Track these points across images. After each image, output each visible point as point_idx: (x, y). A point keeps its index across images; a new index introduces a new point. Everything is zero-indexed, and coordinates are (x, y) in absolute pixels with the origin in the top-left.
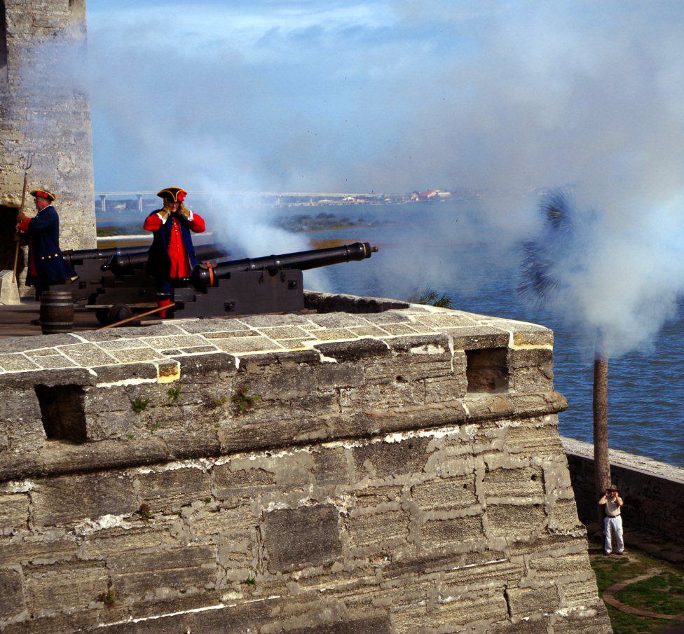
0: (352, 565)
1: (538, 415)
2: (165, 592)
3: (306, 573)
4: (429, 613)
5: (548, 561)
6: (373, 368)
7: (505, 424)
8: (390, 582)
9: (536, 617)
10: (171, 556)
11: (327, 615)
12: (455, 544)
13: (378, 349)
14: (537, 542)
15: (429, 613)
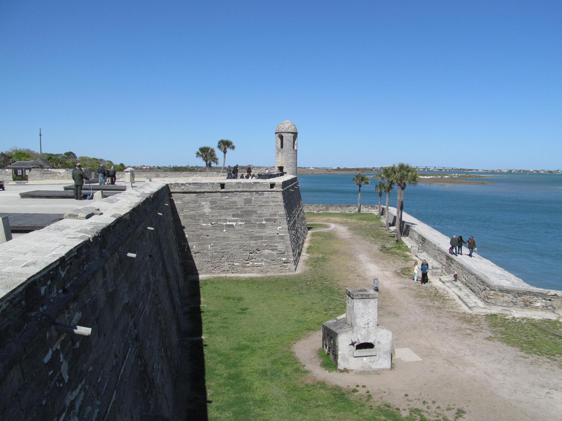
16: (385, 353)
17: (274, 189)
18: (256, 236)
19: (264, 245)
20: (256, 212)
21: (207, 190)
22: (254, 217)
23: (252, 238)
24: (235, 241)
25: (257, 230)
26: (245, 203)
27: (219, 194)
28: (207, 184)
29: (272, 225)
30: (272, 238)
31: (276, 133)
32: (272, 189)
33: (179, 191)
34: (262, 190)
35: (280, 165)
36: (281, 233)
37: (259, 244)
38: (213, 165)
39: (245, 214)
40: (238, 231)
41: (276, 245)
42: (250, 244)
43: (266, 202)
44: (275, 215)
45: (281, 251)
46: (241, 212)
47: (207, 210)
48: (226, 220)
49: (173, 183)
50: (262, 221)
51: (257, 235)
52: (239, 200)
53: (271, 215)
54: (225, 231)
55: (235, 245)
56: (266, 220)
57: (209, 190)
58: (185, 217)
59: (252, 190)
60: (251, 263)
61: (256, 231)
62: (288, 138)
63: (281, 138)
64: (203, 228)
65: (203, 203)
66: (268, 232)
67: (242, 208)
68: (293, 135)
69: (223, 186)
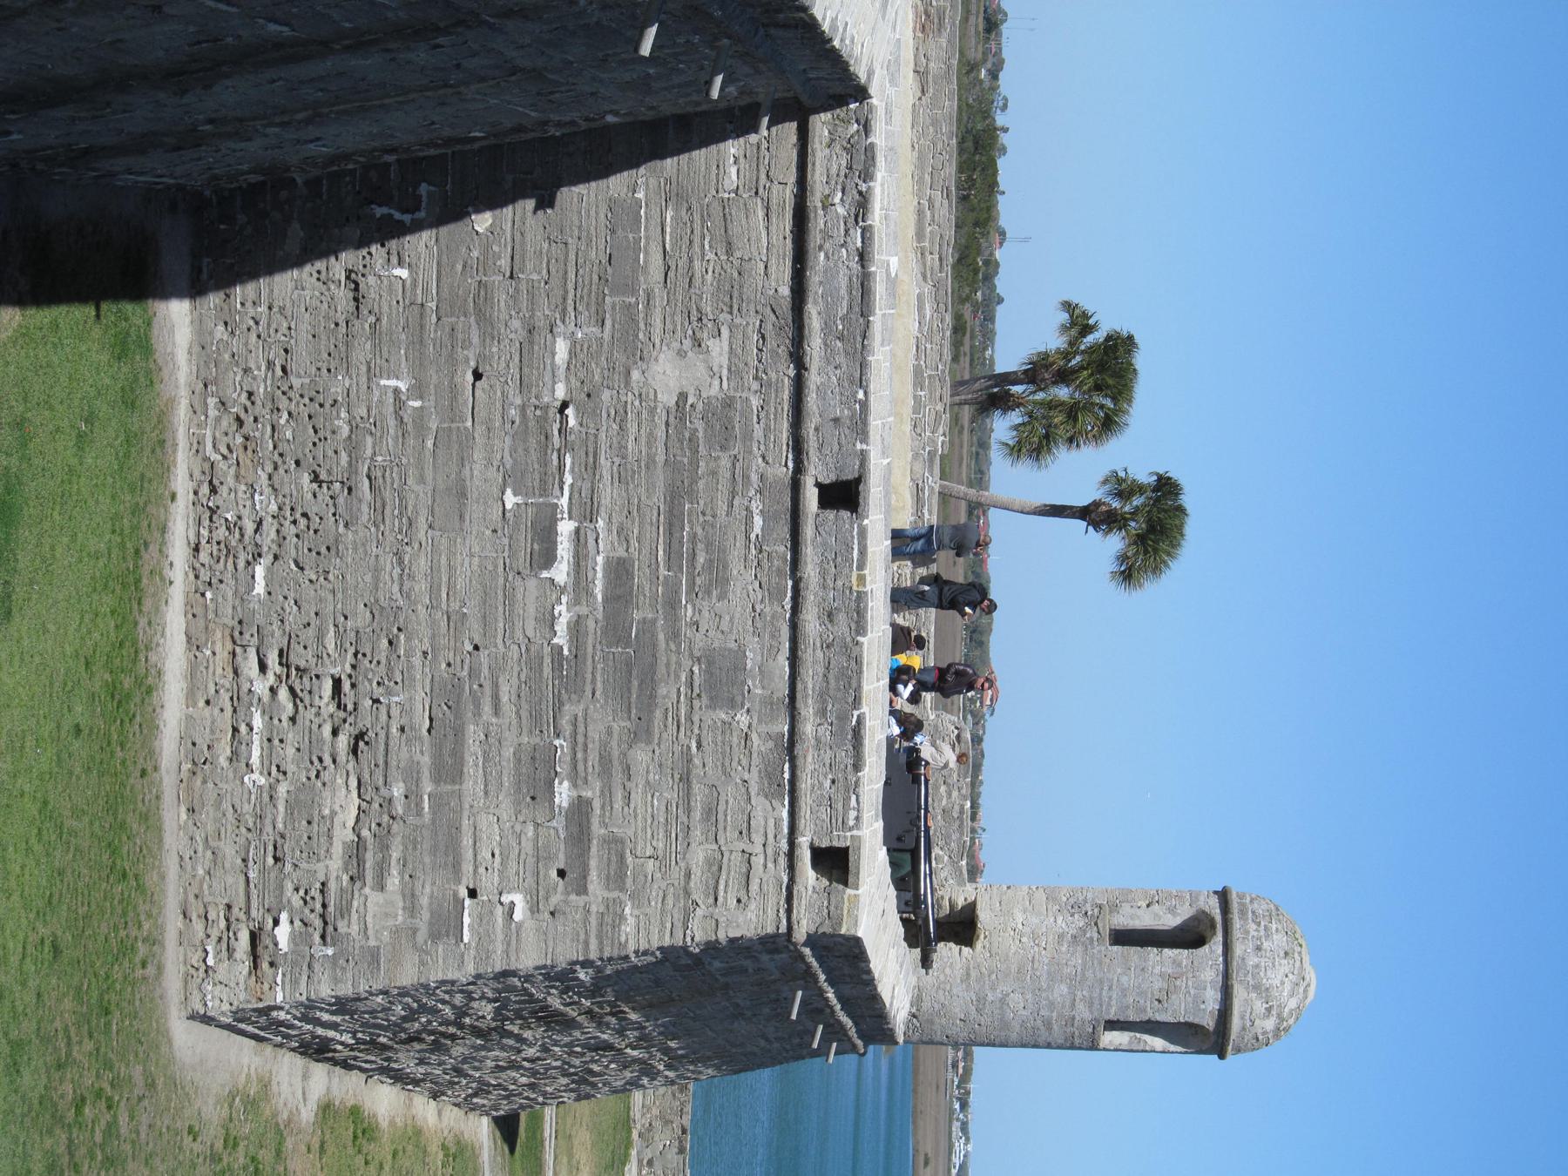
0: (696, 719)
1: (789, 911)
2: (701, 559)
3: (696, 677)
4: (648, 782)
5: (670, 901)
6: (844, 757)
7: (785, 879)
8: (677, 749)
9: (629, 881)
10: (725, 567)
11: (662, 690)
12: (697, 815)
13: (857, 767)
14: (687, 893)
15: (648, 782)
17: (808, 875)
18: (459, 733)
19: (398, 791)
21: (813, 379)
22: (601, 718)
23: (451, 707)
24: (434, 569)
25: (510, 738)
26: (709, 659)
27: (782, 471)
28: (862, 383)
29: (541, 856)
31: (1223, 896)
32: (805, 856)
33: (817, 177)
34: (805, 784)
35: (984, 917)
36: (482, 918)
37: (401, 754)
38: (1003, 426)
39: (627, 652)
40: (509, 597)
41: (394, 881)
42: (407, 682)
43: (710, 812)
44: (616, 878)
45: (344, 911)
46: (647, 626)
47: (667, 375)
48: (586, 511)
49: (878, 138)
50: (575, 779)
52: (738, 613)
53: (615, 845)
54: (511, 500)
55: (406, 574)
56: (580, 811)
57: (811, 400)
58: (623, 216)
59: (808, 710)
60: (261, 687)
61: (495, 735)
62: (1190, 983)
63: (1191, 936)
64: (534, 337)
65: (719, 349)
66: (492, 824)
67: (675, 635)
68: (1209, 1023)
69: (844, 495)
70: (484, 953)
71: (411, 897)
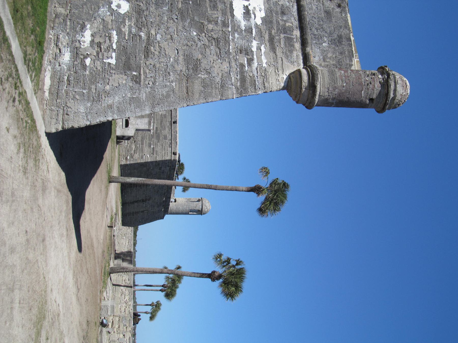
16: (123, 132)
17: (173, 155)
20: (158, 142)
22: (155, 140)
26: (164, 136)
30: (142, 151)
36: (145, 157)
37: (138, 142)
39: (157, 135)
44: (157, 154)
48: (154, 123)
51: (144, 141)
52: (166, 132)
53: (157, 151)
56: (153, 148)
59: (173, 140)
61: (146, 141)
63: (199, 201)
66: (146, 149)
70: (145, 160)
71: (139, 155)
